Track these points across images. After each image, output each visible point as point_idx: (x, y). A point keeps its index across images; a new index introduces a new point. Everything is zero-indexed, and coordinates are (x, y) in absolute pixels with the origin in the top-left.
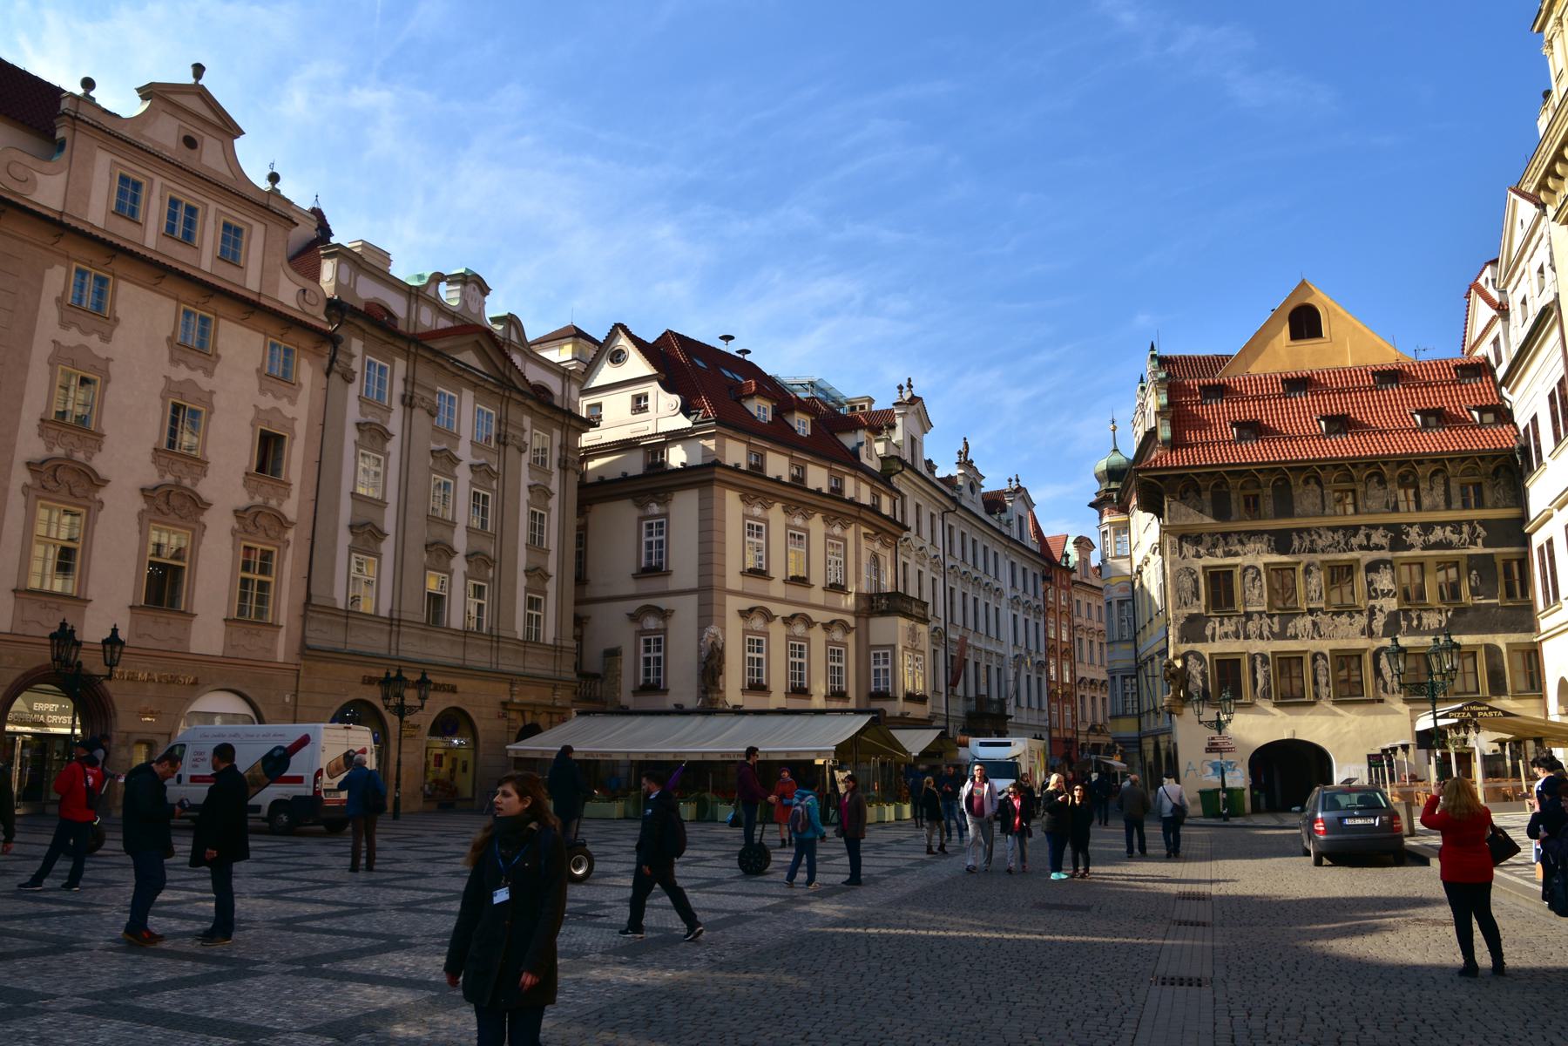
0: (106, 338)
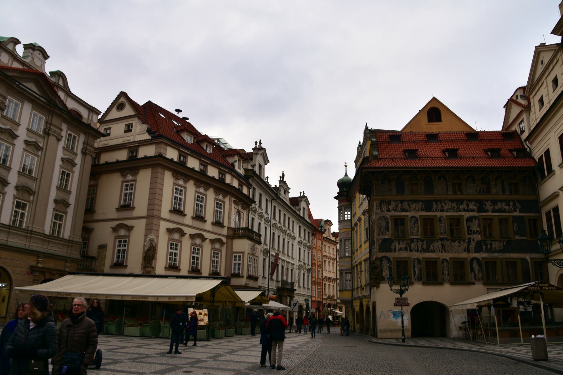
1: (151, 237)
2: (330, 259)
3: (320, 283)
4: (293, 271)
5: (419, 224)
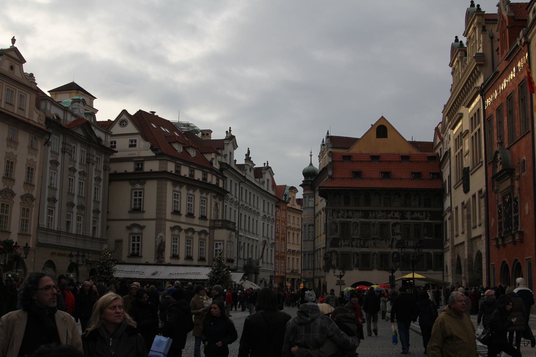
1: (161, 235)
2: (295, 230)
3: (284, 257)
4: (258, 248)
5: (359, 227)
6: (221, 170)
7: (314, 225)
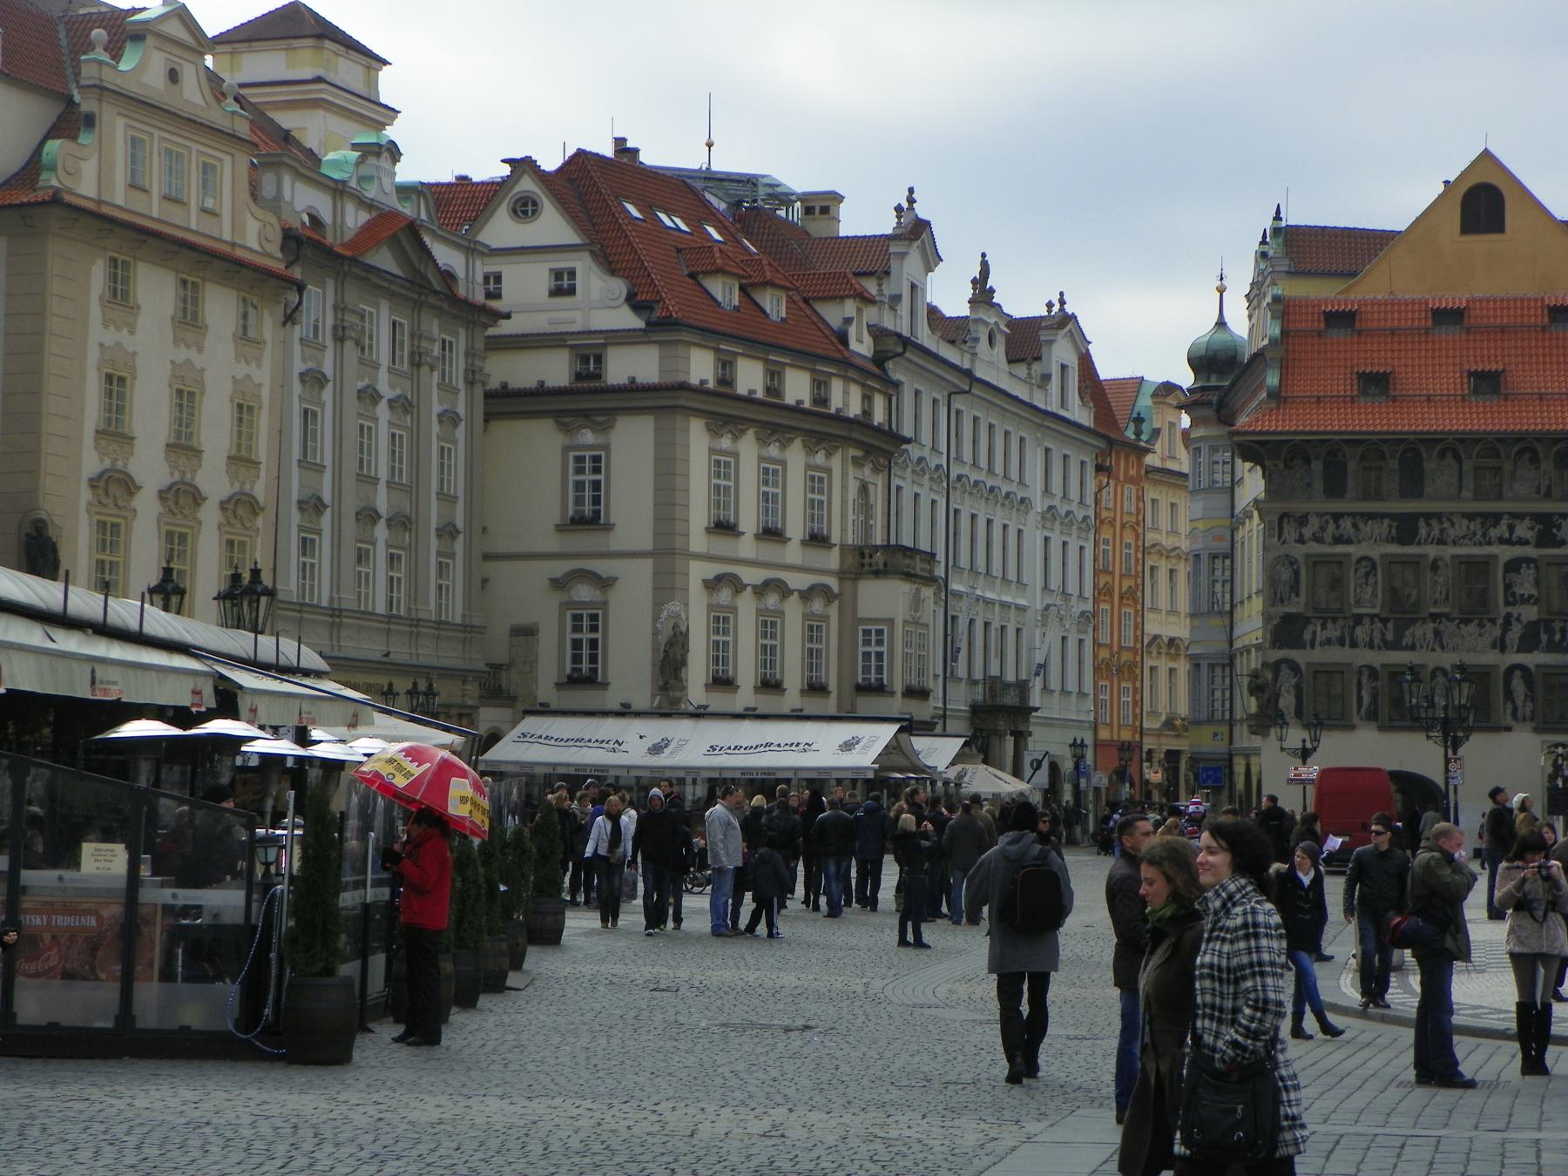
0: (132, 332)
2: (1178, 557)
3: (1132, 666)
4: (1024, 633)
6: (880, 359)
7: (1230, 556)
